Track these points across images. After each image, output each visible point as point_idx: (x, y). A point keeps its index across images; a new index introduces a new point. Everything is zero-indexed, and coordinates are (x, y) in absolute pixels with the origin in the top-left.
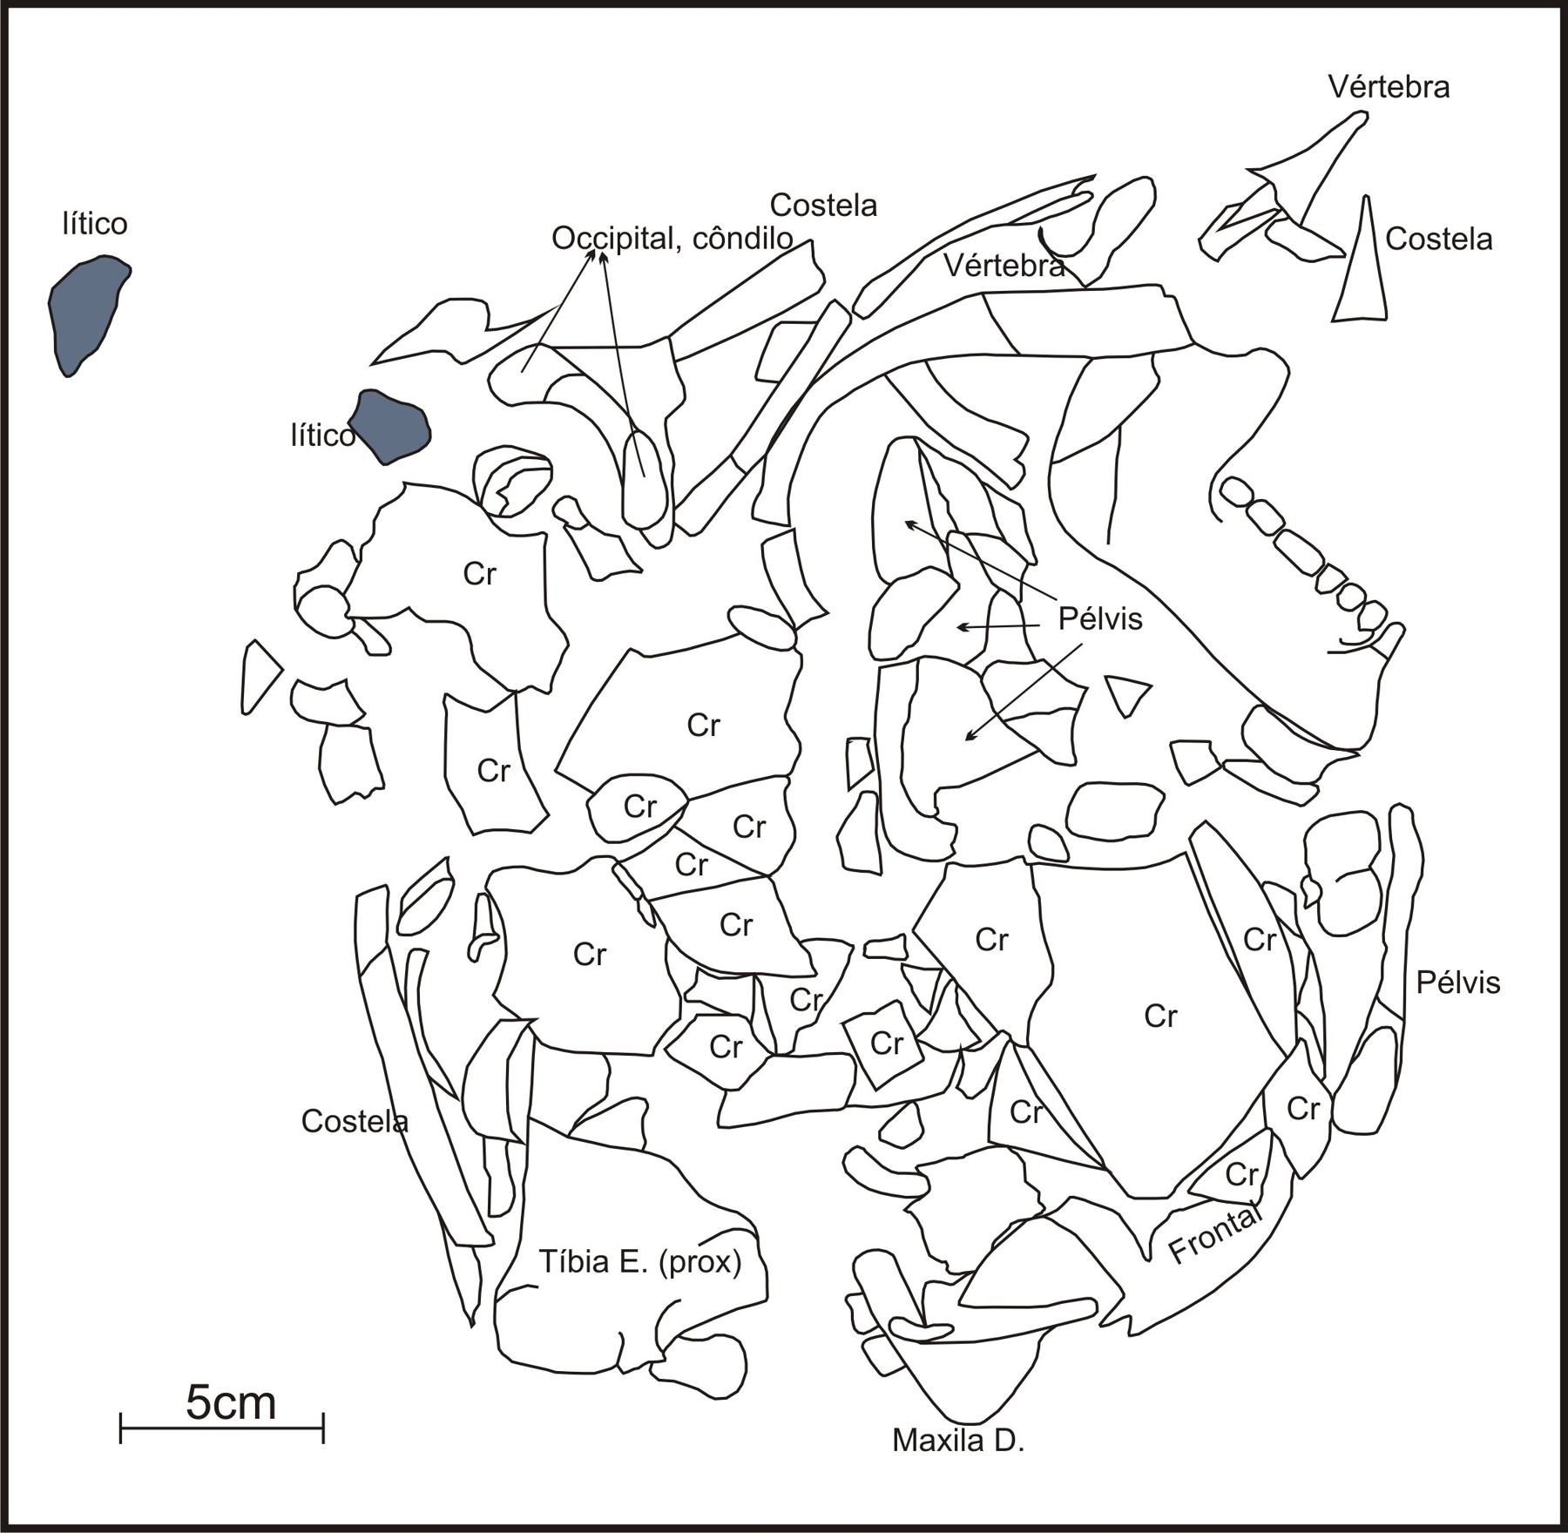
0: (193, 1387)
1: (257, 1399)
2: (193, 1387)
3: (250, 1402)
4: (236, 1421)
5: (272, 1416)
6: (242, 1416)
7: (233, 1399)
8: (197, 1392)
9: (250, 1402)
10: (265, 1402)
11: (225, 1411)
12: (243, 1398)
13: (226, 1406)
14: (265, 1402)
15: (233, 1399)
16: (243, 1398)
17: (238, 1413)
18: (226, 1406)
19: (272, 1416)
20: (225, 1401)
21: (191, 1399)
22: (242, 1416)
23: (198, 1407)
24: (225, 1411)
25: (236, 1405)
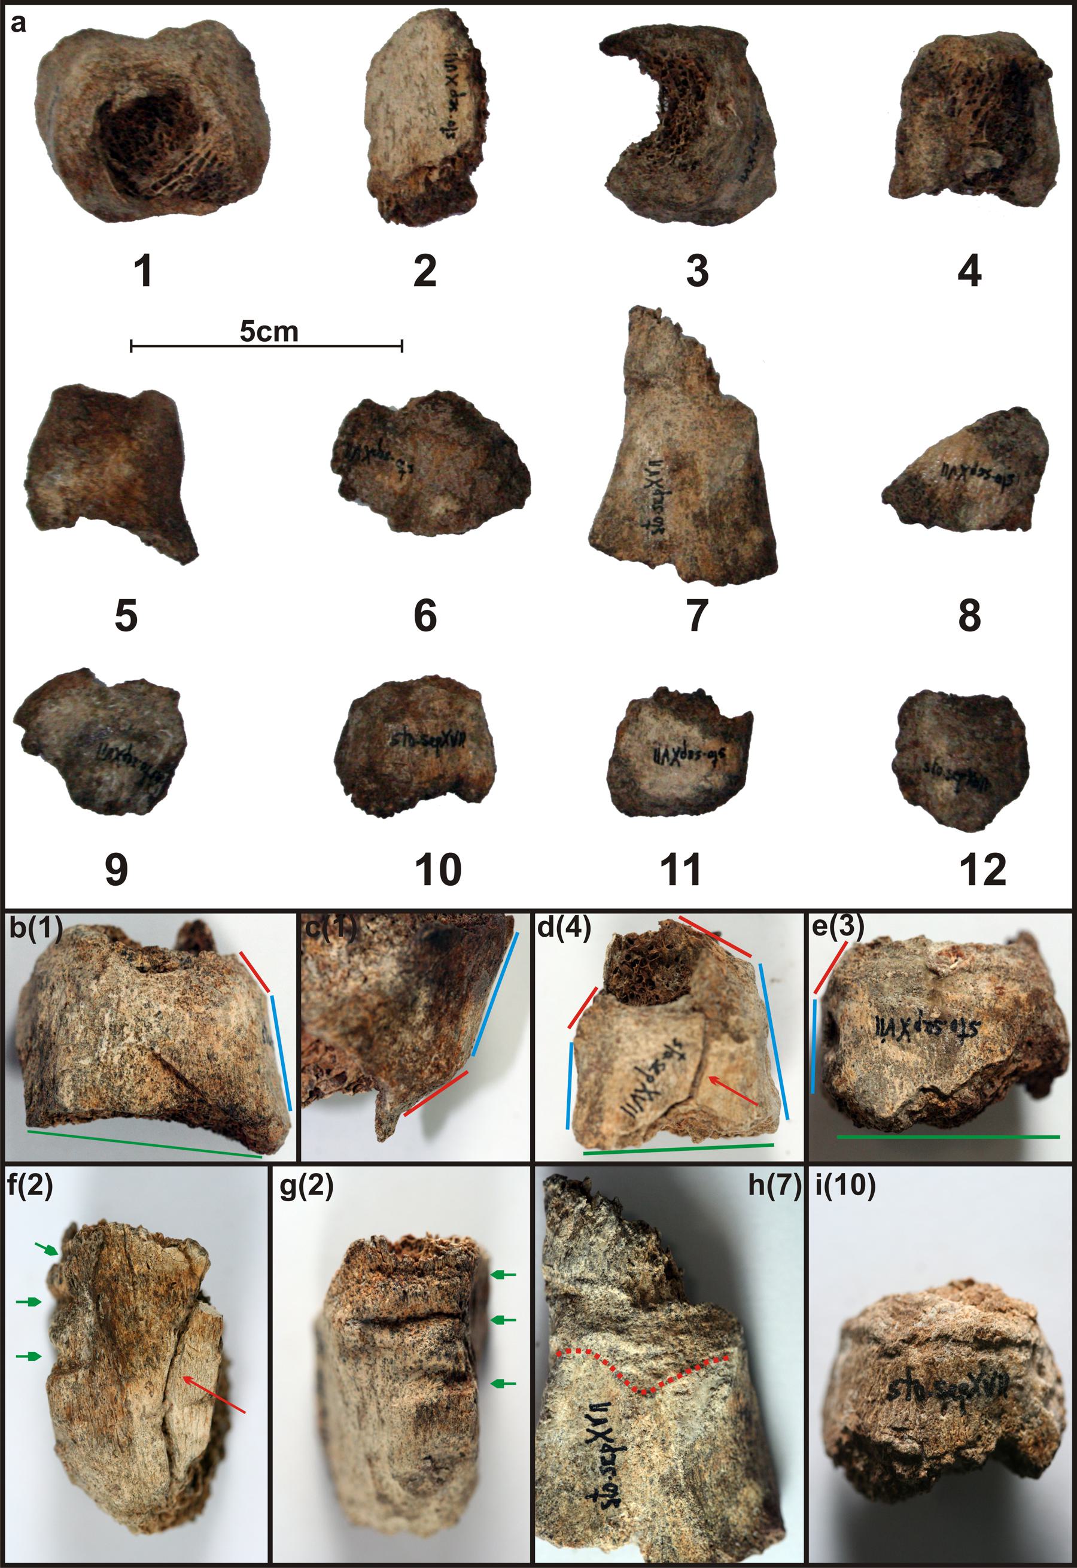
0: (245, 322)
2: (245, 322)
3: (281, 332)
4: (272, 342)
5: (295, 339)
8: (247, 325)
9: (281, 332)
10: (291, 332)
13: (265, 333)
14: (291, 332)
16: (277, 329)
18: (265, 333)
19: (295, 339)
21: (244, 329)
23: (247, 334)
25: (272, 333)
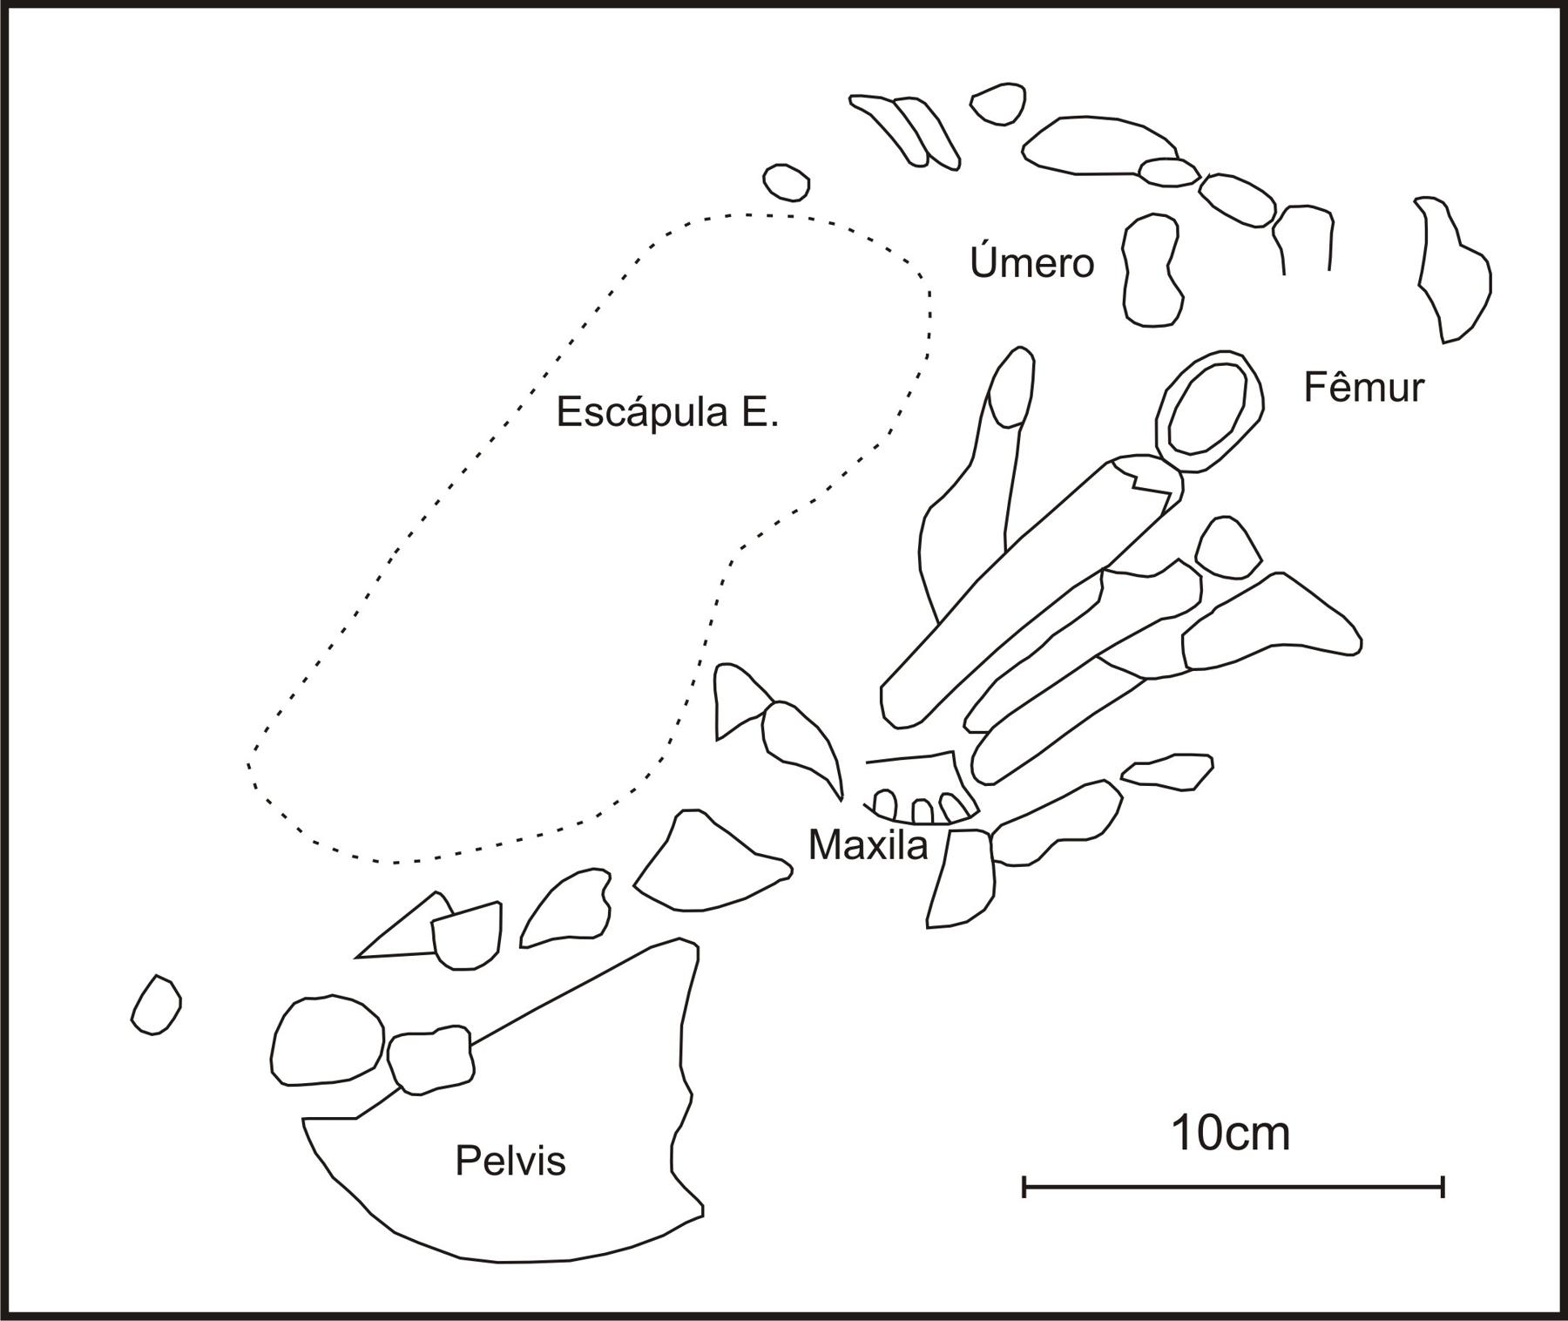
1: (1271, 1129)
3: (1263, 1132)
6: (1255, 1147)
7: (1246, 1129)
9: (1263, 1132)
10: (1279, 1132)
11: (1237, 1142)
12: (1256, 1128)
13: (1239, 1136)
14: (1279, 1132)
15: (1246, 1129)
16: (1256, 1128)
17: (1251, 1144)
20: (1237, 1131)
22: (1255, 1147)
24: (1237, 1142)
25: (1249, 1136)
